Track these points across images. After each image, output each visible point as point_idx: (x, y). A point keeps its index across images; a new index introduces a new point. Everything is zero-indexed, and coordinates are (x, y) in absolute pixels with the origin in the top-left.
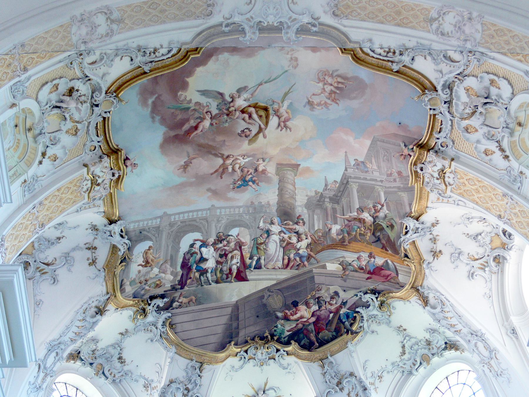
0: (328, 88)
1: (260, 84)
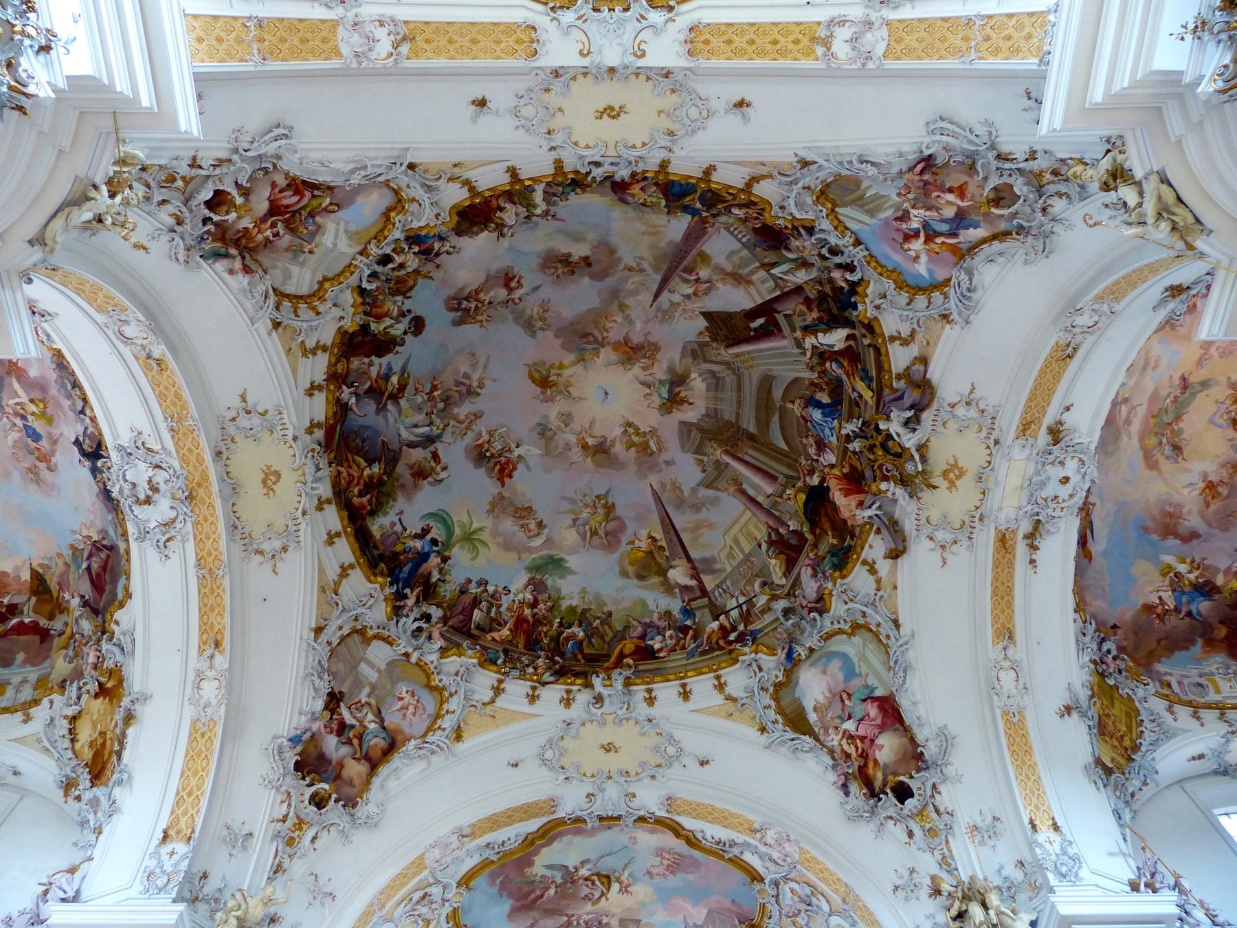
0: (666, 862)
1: (602, 857)
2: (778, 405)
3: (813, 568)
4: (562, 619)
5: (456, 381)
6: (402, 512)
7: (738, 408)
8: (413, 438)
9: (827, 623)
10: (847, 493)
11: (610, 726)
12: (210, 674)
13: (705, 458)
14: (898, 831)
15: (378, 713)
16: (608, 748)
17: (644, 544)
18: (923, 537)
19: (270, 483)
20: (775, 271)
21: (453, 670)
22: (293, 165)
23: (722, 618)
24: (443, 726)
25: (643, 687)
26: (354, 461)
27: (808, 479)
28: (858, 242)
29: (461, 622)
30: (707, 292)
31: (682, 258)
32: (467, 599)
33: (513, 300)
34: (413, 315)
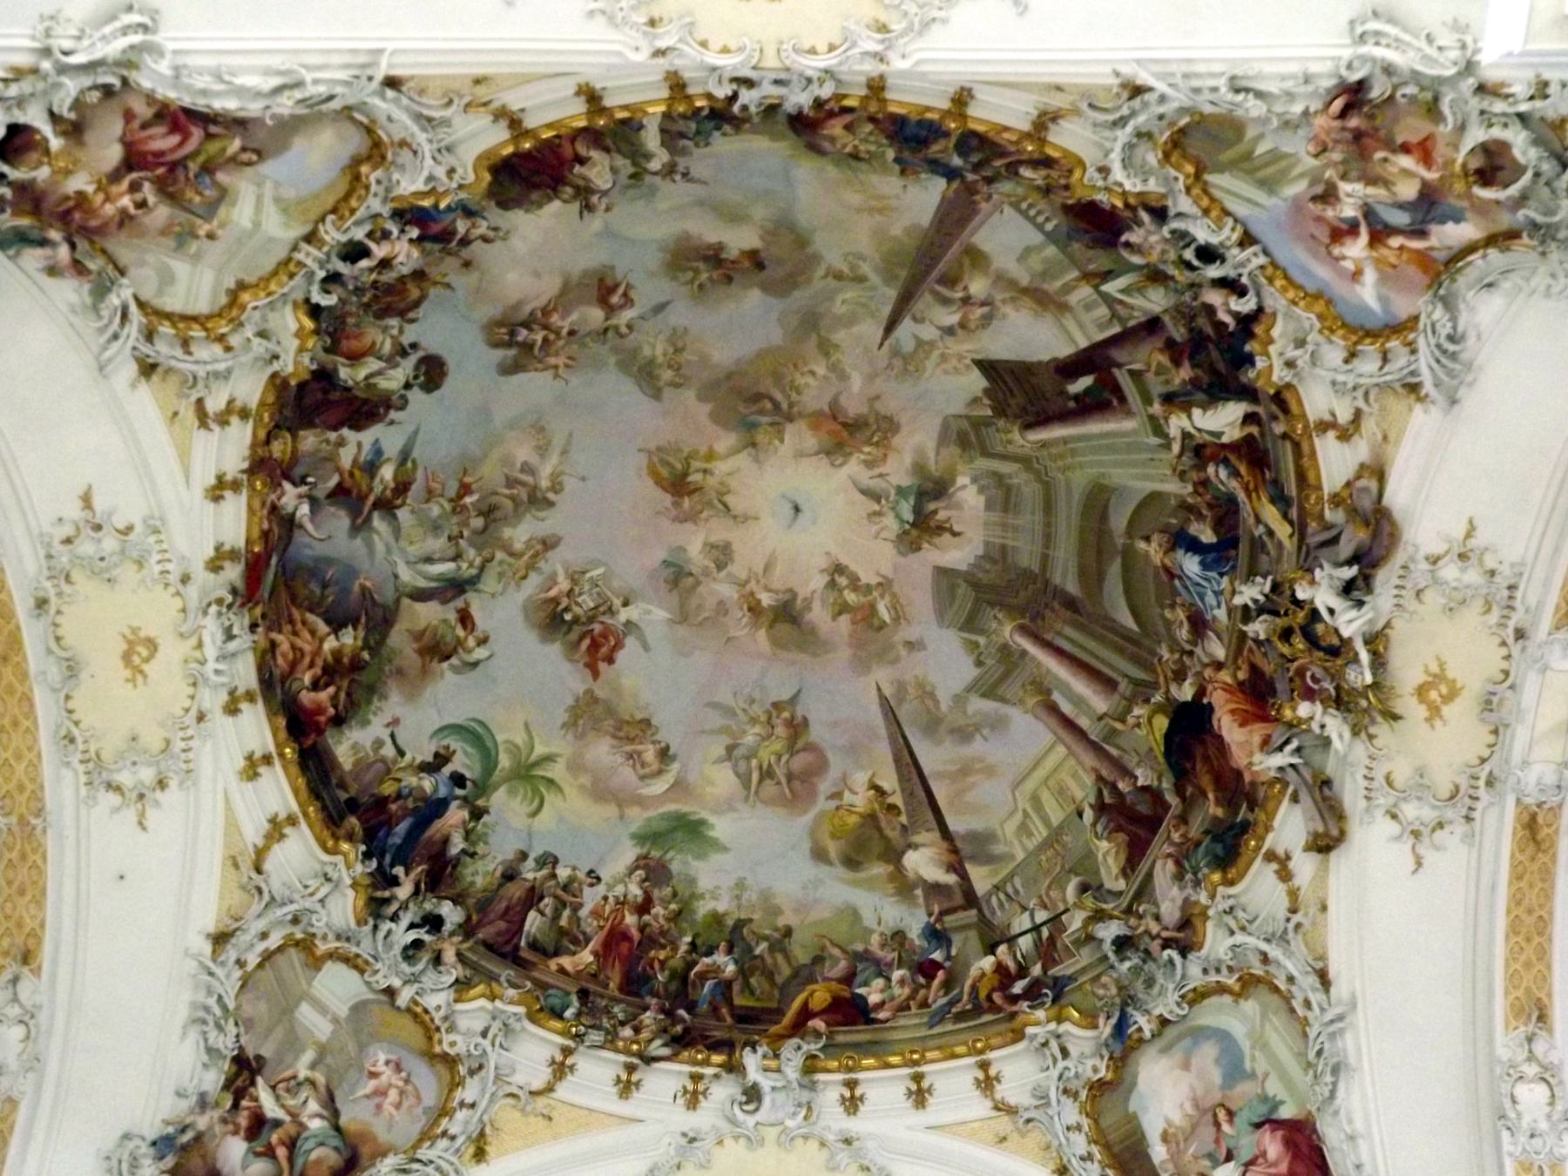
2: (1120, 541)
3: (1178, 863)
4: (695, 937)
5: (507, 478)
6: (396, 722)
7: (1047, 545)
8: (422, 583)
9: (1194, 970)
13: (982, 640)
17: (860, 799)
18: (1379, 813)
19: (136, 660)
20: (1111, 287)
21: (479, 1026)
22: (155, 78)
23: (1002, 949)
24: (452, 1131)
25: (840, 1077)
26: (304, 623)
27: (1173, 689)
28: (1247, 240)
29: (499, 934)
30: (987, 320)
31: (935, 261)
32: (515, 891)
33: (616, 328)
34: (420, 354)
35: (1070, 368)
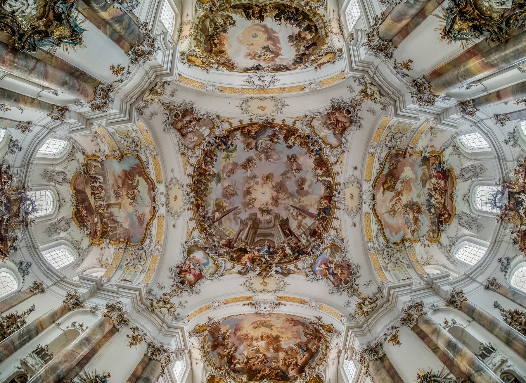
10: (248, 258)
11: (182, 198)
12: (214, 88)
14: (172, 283)
15: (192, 132)
16: (176, 198)
17: (224, 205)
20: (303, 235)
28: (321, 253)
32: (213, 156)
35: (289, 230)
